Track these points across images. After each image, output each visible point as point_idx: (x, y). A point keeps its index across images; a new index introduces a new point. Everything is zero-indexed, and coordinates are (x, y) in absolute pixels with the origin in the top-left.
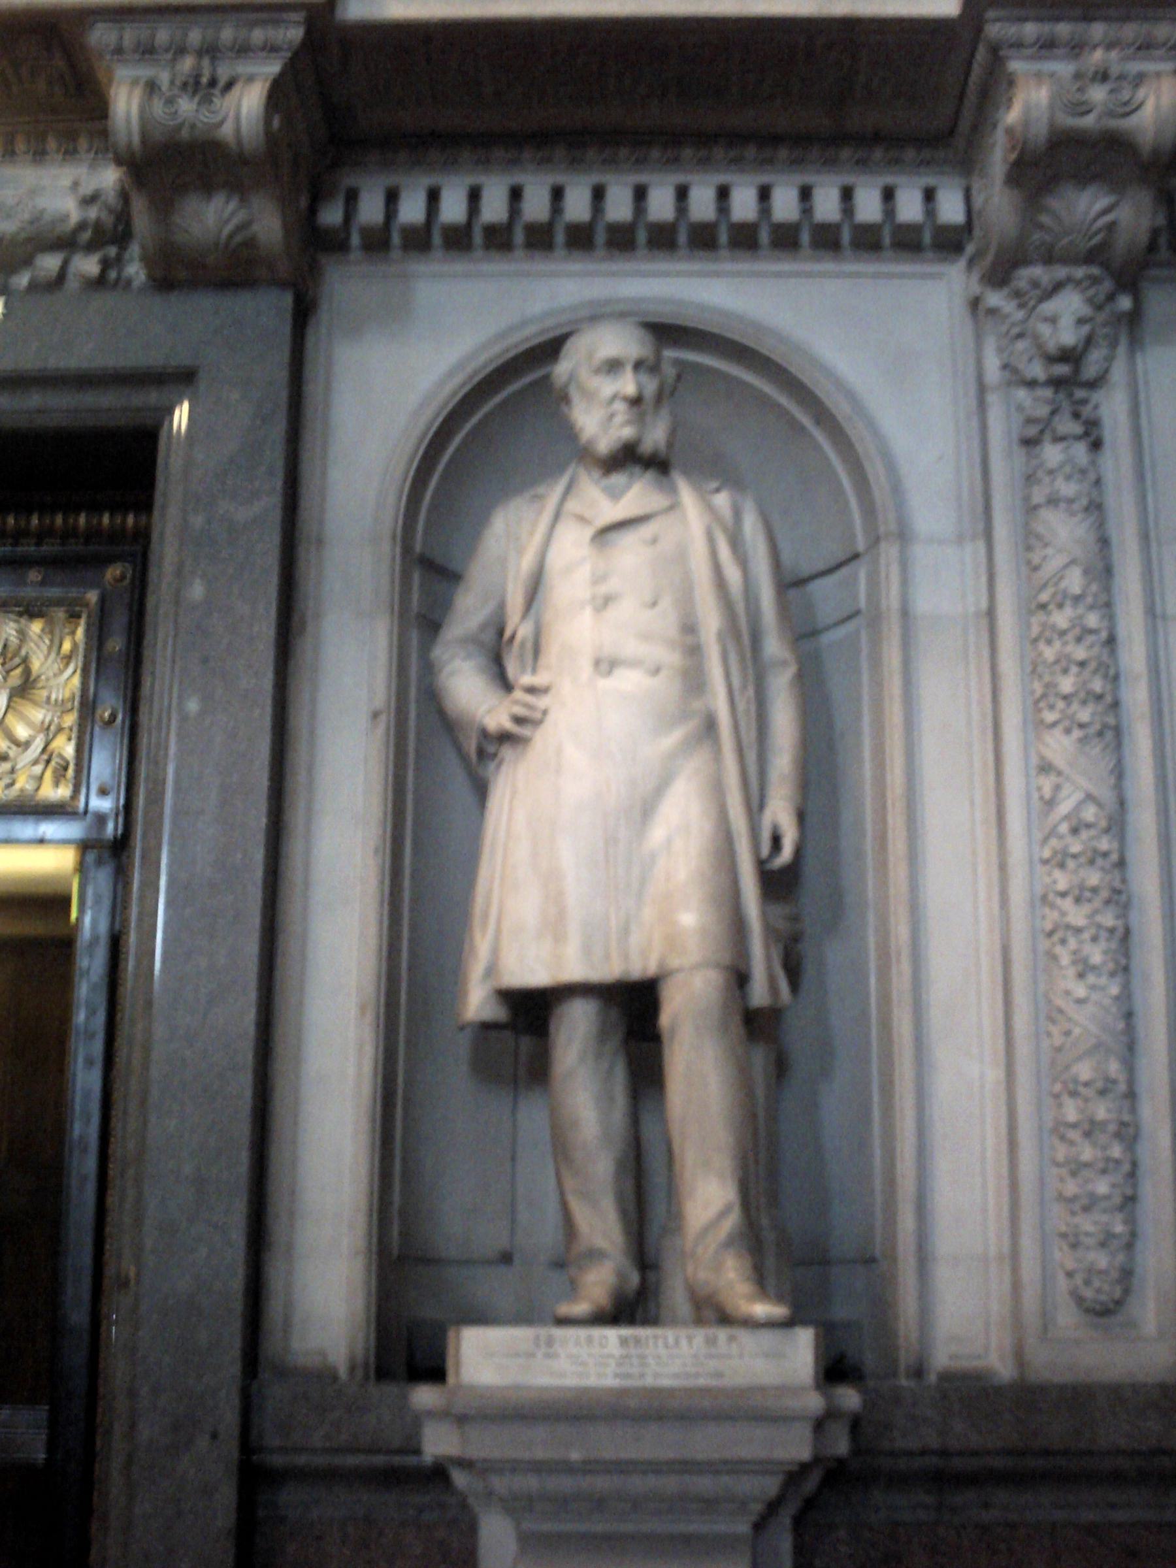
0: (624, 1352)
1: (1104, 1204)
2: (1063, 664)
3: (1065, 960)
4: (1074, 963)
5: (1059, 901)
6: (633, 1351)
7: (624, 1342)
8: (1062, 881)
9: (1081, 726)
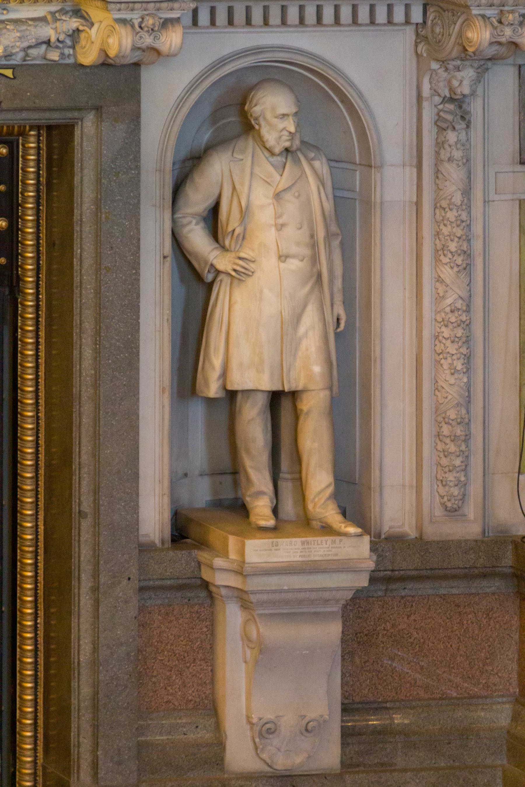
0: (303, 547)
1: (458, 469)
2: (451, 236)
3: (446, 367)
4: (450, 368)
5: (444, 341)
6: (306, 546)
7: (303, 543)
8: (446, 332)
9: (458, 266)
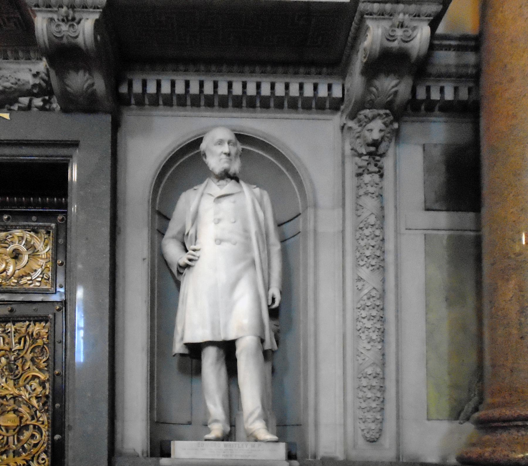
5: (362, 320)
9: (372, 266)
